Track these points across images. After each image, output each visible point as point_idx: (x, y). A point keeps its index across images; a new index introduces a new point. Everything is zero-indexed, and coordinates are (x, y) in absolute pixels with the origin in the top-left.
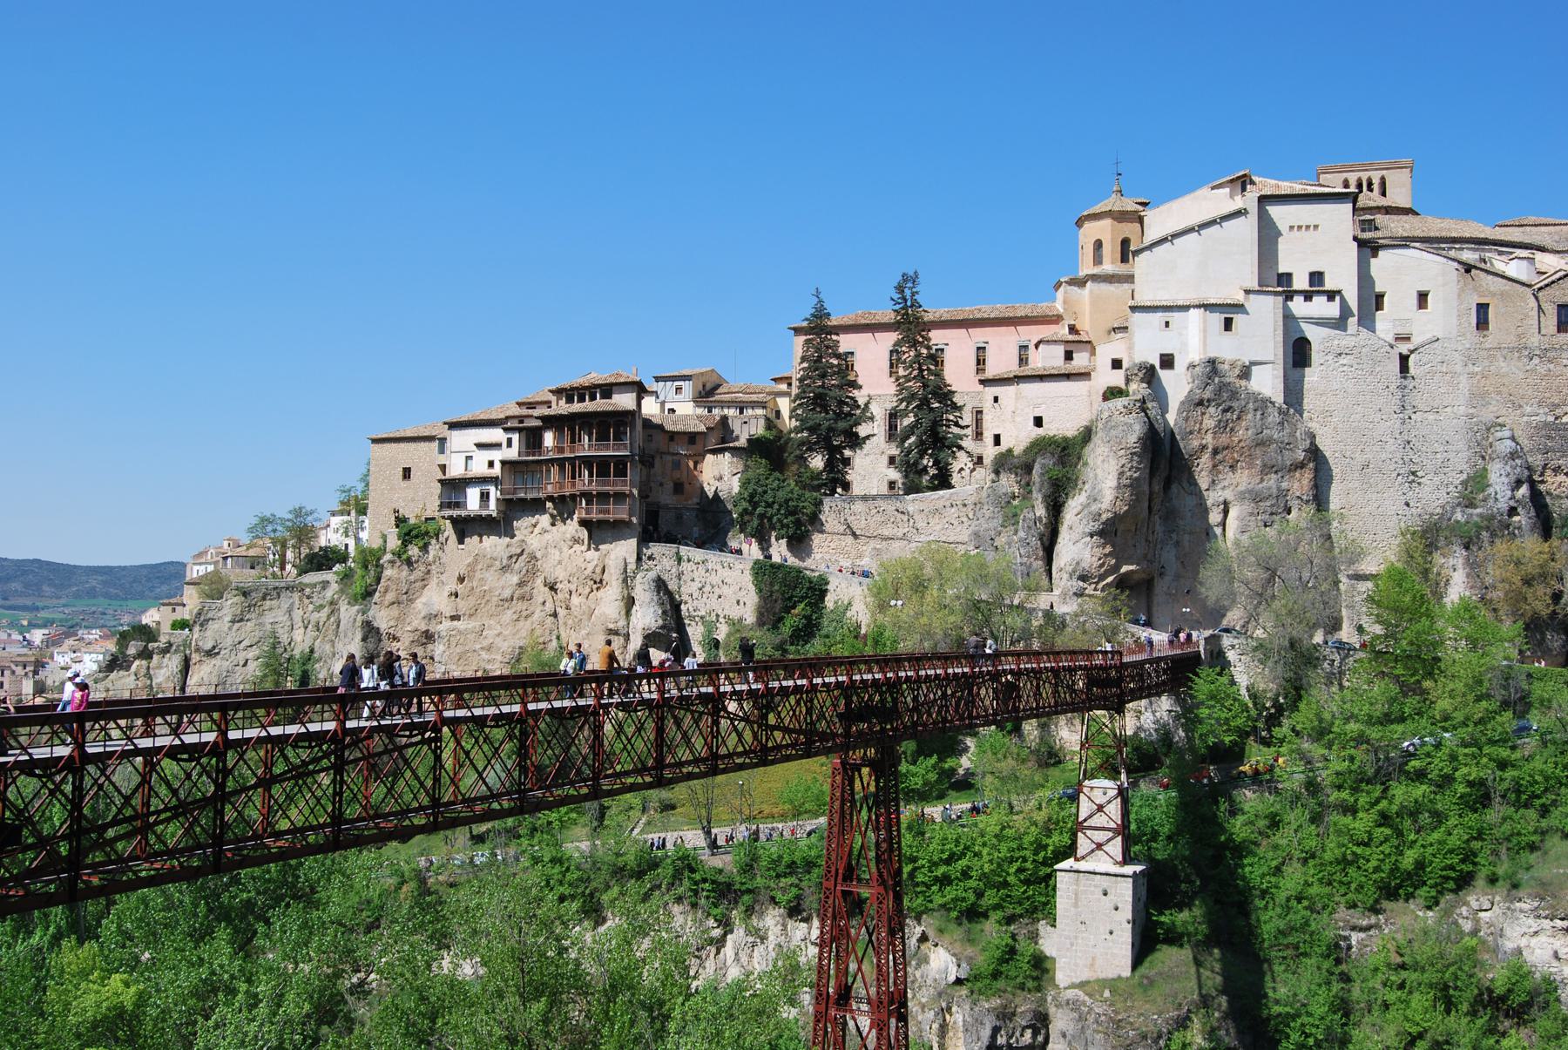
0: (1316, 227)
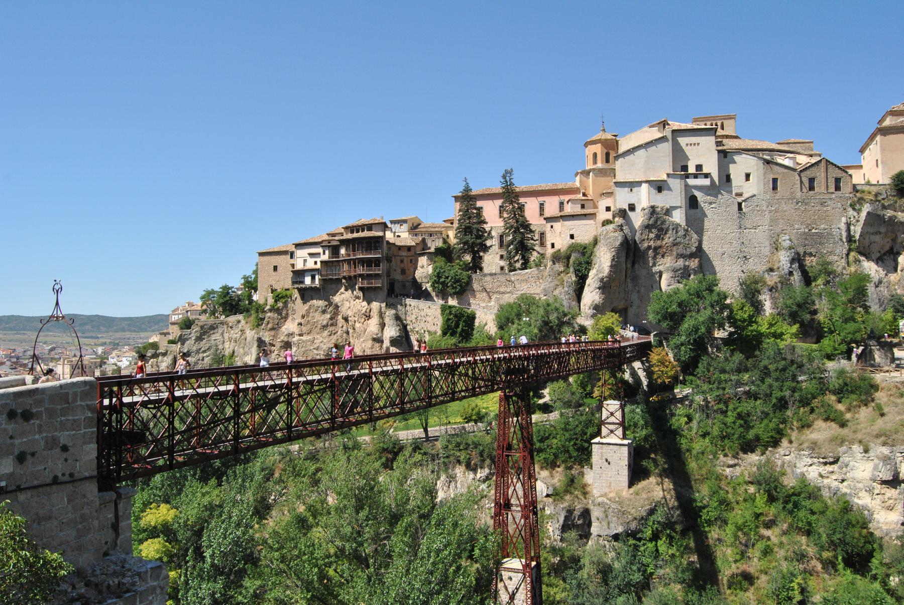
0: (698, 144)
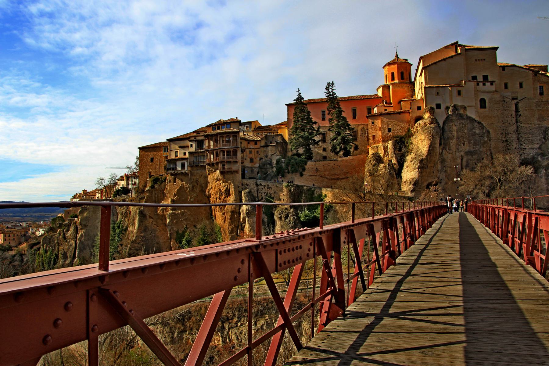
0: (484, 60)
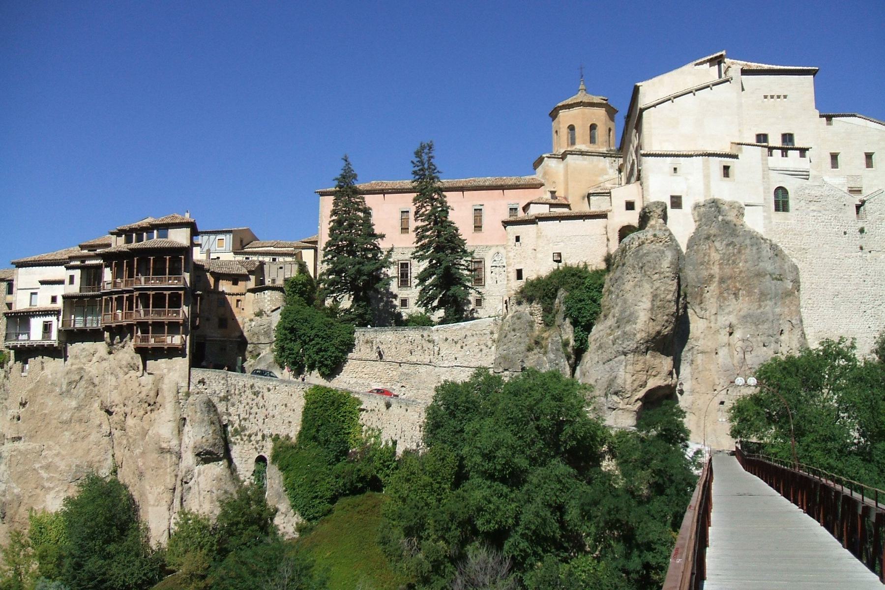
0: (785, 97)
